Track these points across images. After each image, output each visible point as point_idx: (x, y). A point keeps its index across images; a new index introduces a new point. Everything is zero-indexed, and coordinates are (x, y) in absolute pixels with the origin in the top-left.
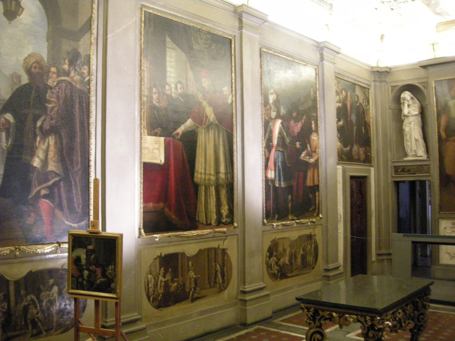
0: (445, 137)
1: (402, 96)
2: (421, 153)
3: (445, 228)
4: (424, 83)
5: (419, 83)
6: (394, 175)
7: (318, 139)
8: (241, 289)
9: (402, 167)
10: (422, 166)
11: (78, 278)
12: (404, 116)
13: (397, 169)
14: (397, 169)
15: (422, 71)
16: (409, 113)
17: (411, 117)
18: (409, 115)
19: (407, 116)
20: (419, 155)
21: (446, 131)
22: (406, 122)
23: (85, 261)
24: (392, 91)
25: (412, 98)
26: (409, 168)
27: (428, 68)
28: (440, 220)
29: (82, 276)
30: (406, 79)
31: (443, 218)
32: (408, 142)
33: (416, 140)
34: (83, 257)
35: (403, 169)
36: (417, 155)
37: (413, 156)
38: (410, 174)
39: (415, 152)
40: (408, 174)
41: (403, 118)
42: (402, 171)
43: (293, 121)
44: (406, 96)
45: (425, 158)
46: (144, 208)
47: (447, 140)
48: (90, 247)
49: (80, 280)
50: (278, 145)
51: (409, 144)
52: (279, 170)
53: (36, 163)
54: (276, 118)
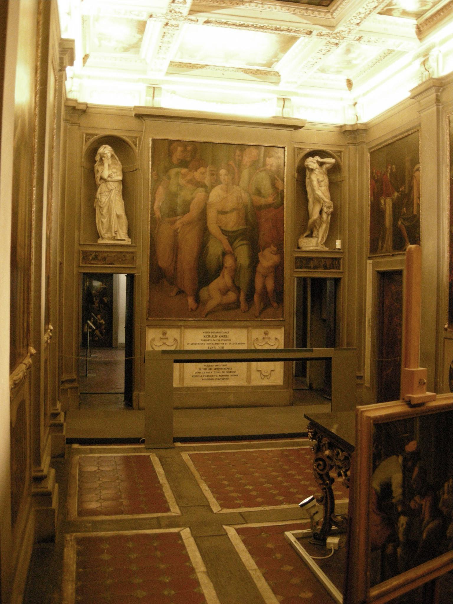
0: (160, 217)
1: (101, 150)
2: (122, 234)
3: (153, 339)
4: (136, 138)
5: (129, 137)
6: (81, 265)
8: (33, 474)
9: (94, 254)
10: (124, 254)
11: (384, 547)
12: (102, 178)
13: (85, 256)
14: (85, 256)
15: (135, 122)
16: (109, 176)
17: (111, 183)
18: (109, 179)
19: (105, 181)
20: (119, 238)
22: (102, 188)
23: (400, 490)
24: (86, 141)
25: (112, 156)
26: (106, 255)
27: (145, 119)
28: (147, 328)
29: (393, 538)
31: (151, 326)
32: (104, 218)
33: (118, 217)
34: (397, 478)
36: (116, 238)
37: (109, 239)
38: (106, 264)
39: (116, 233)
40: (103, 264)
41: (98, 181)
42: (93, 259)
44: (107, 152)
45: (130, 243)
48: (411, 447)
49: (390, 549)
51: (105, 221)
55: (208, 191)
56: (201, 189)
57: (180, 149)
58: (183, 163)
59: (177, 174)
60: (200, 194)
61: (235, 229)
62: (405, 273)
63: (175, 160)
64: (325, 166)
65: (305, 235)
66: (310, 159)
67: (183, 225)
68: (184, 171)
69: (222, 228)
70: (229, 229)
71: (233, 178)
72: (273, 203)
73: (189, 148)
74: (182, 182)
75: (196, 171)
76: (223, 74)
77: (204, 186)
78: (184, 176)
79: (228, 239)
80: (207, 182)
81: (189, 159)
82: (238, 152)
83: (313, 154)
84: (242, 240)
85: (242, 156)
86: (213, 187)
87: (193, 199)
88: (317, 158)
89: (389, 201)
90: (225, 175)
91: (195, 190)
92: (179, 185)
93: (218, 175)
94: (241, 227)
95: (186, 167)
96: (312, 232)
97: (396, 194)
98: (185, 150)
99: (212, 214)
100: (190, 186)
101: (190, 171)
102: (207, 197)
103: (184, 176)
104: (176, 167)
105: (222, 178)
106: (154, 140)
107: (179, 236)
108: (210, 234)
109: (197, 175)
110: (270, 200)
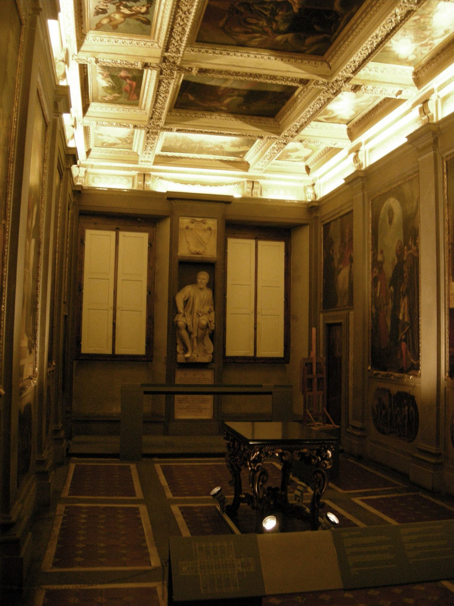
46: (450, 352)
53: (401, 317)
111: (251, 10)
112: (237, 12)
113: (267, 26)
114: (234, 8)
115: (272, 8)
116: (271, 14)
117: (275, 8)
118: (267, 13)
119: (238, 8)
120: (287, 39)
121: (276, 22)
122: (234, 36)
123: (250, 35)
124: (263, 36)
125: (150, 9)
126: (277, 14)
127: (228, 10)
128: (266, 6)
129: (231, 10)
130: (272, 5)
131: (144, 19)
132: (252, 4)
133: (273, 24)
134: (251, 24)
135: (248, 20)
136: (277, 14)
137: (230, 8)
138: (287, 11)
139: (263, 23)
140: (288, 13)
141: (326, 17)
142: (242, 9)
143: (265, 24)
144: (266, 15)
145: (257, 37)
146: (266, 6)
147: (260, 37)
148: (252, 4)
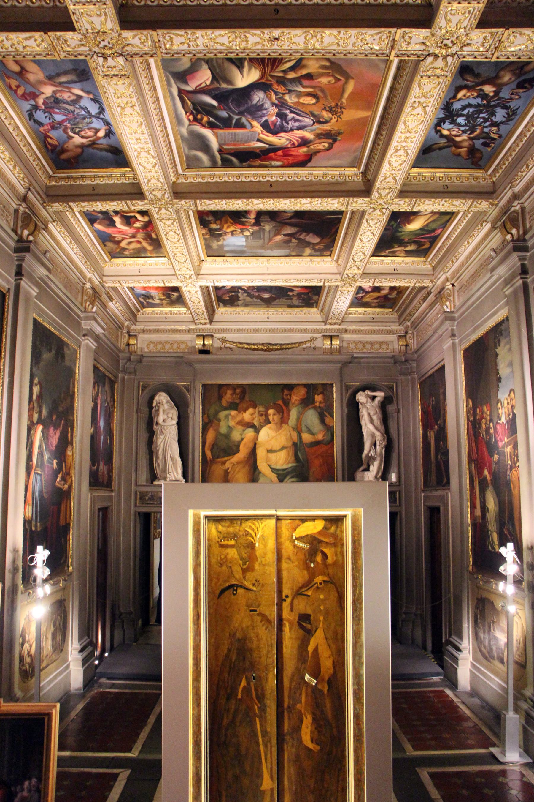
7: (73, 455)
9: (150, 494)
21: (212, 450)
30: (164, 377)
35: (152, 496)
43: (52, 428)
44: (162, 398)
47: (213, 461)
50: (37, 466)
52: (36, 503)
54: (37, 423)
55: (257, 430)
56: (251, 430)
57: (229, 392)
58: (233, 406)
59: (227, 416)
60: (250, 433)
61: (285, 467)
62: (442, 509)
63: (224, 403)
64: (377, 400)
65: (361, 469)
66: (361, 393)
67: (234, 465)
68: (233, 413)
69: (273, 467)
70: (278, 467)
71: (282, 418)
72: (323, 440)
73: (238, 391)
74: (232, 423)
75: (245, 412)
76: (268, 318)
77: (253, 426)
78: (233, 418)
79: (278, 477)
80: (256, 423)
81: (237, 401)
82: (286, 392)
83: (363, 389)
84: (292, 477)
85: (290, 396)
86: (262, 427)
87: (242, 439)
88: (367, 392)
89: (432, 434)
90: (274, 414)
91: (244, 430)
92: (229, 427)
93: (267, 415)
94: (290, 465)
95: (236, 409)
96: (369, 466)
97: (436, 427)
98: (234, 393)
99: (261, 453)
100: (240, 428)
101: (239, 412)
102: (257, 438)
103: (233, 418)
104: (226, 409)
105: (271, 418)
106: (204, 386)
107: (230, 475)
108: (260, 472)
109: (247, 416)
110: (320, 437)
111: (313, 115)
112: (331, 110)
113: (284, 94)
114: (336, 114)
115: (288, 124)
116: (286, 115)
117: (285, 124)
118: (291, 116)
119: (330, 115)
120: (242, 73)
121: (273, 104)
122: (328, 64)
123: (304, 72)
124: (281, 75)
125: (452, 95)
126: (277, 115)
127: (343, 110)
128: (297, 124)
129: (339, 110)
130: (290, 126)
131: (468, 77)
132: (314, 123)
133: (276, 99)
134: (309, 94)
135: (314, 101)
136: (277, 115)
137: (342, 113)
138: (266, 121)
139: (290, 97)
140: (264, 119)
141: (211, 119)
142: (326, 115)
143: (287, 97)
144: (292, 112)
145: (293, 69)
146: (297, 124)
147: (284, 72)
148: (314, 123)
